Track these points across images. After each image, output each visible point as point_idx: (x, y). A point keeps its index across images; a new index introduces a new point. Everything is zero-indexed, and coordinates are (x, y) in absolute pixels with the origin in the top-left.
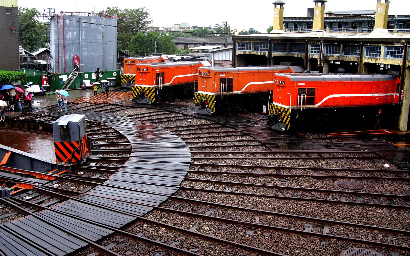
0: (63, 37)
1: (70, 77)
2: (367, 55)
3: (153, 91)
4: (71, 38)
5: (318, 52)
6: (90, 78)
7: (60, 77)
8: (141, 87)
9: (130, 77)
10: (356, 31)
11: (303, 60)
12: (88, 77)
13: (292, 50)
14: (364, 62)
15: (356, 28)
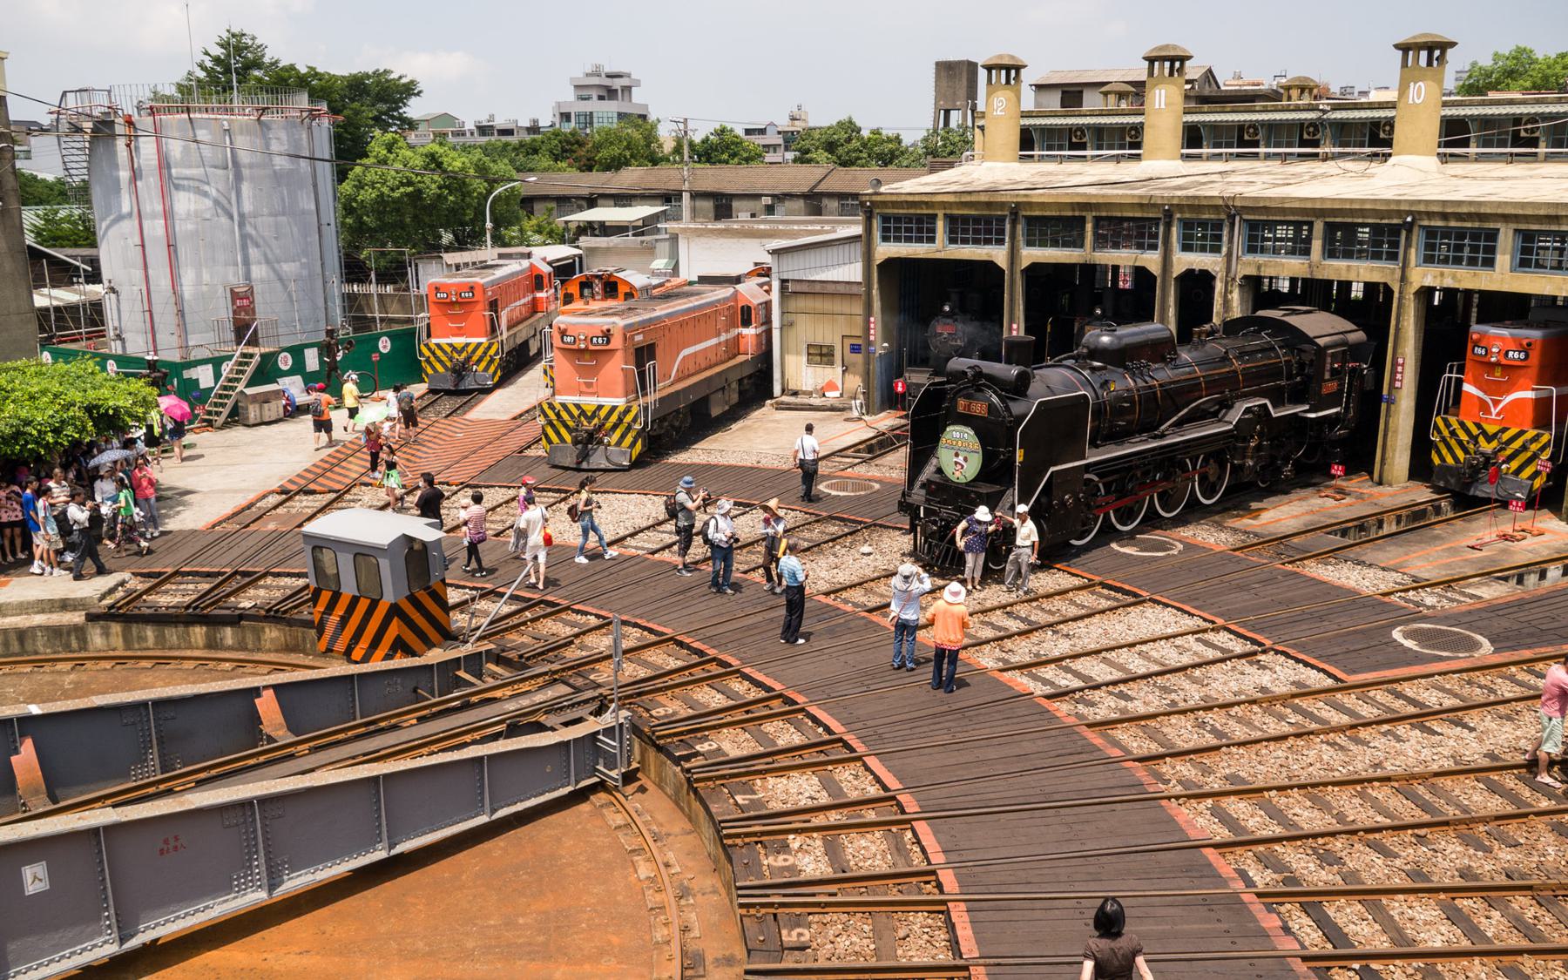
0: (159, 208)
1: (226, 368)
2: (1429, 260)
3: (629, 418)
4: (196, 211)
5: (1216, 249)
6: (298, 368)
7: (186, 374)
8: (578, 406)
9: (460, 352)
10: (1256, 155)
11: (1155, 278)
12: (290, 362)
13: (1100, 242)
14: (1415, 287)
15: (1256, 144)
